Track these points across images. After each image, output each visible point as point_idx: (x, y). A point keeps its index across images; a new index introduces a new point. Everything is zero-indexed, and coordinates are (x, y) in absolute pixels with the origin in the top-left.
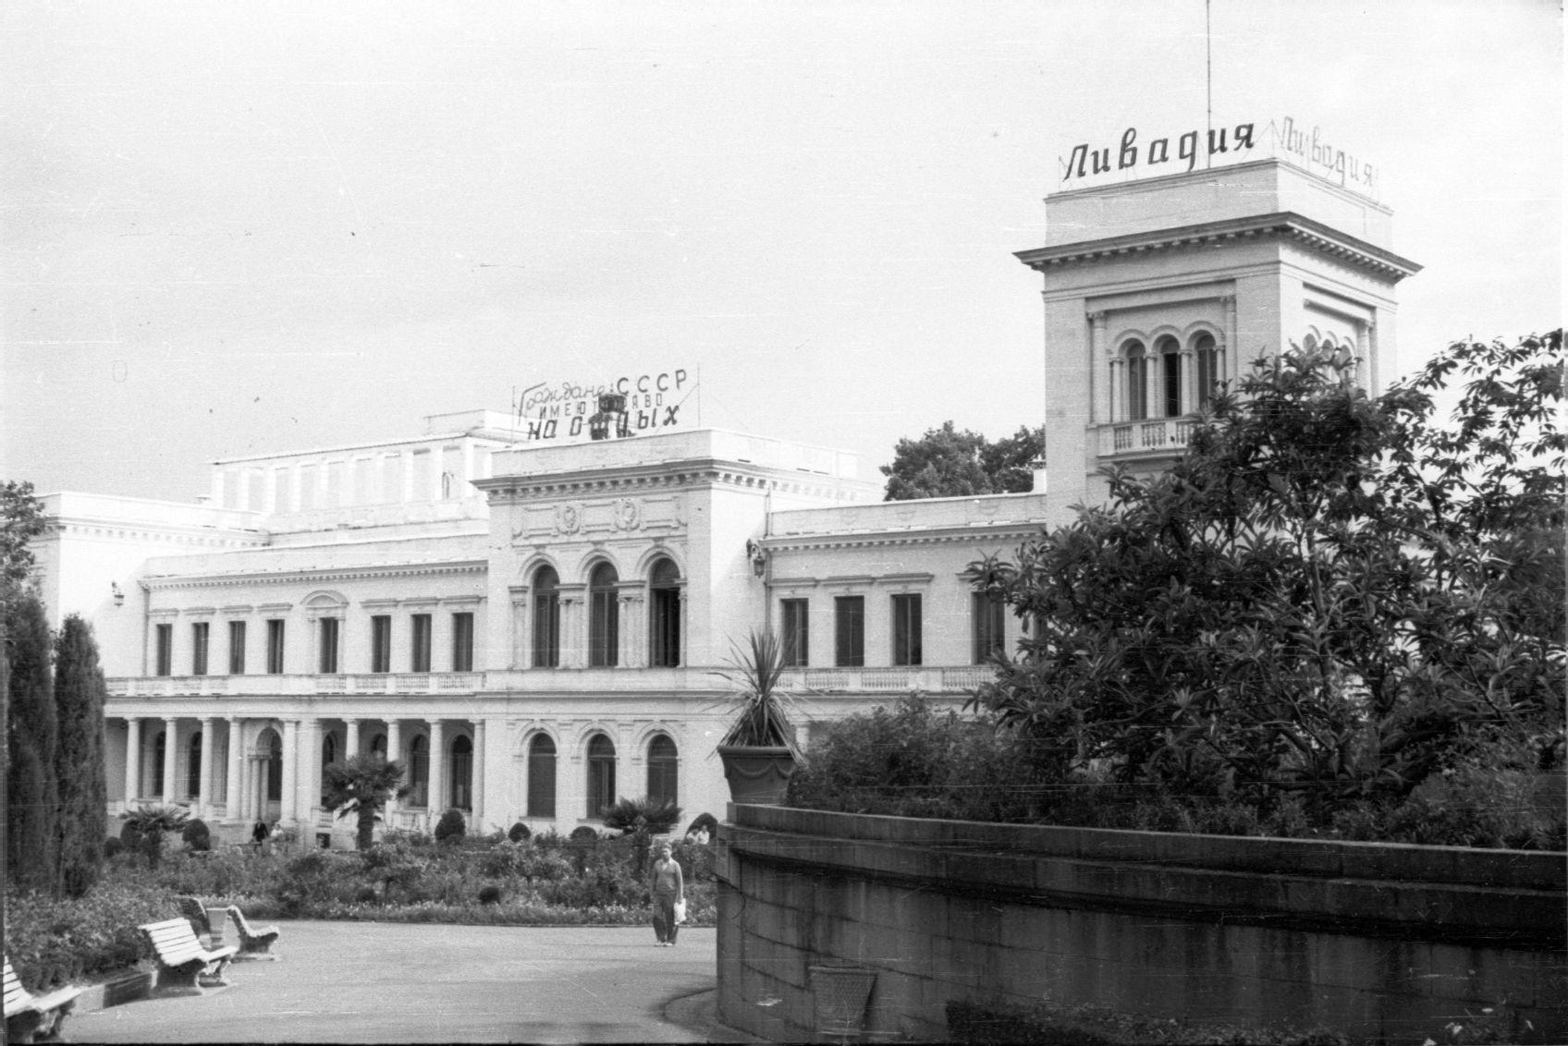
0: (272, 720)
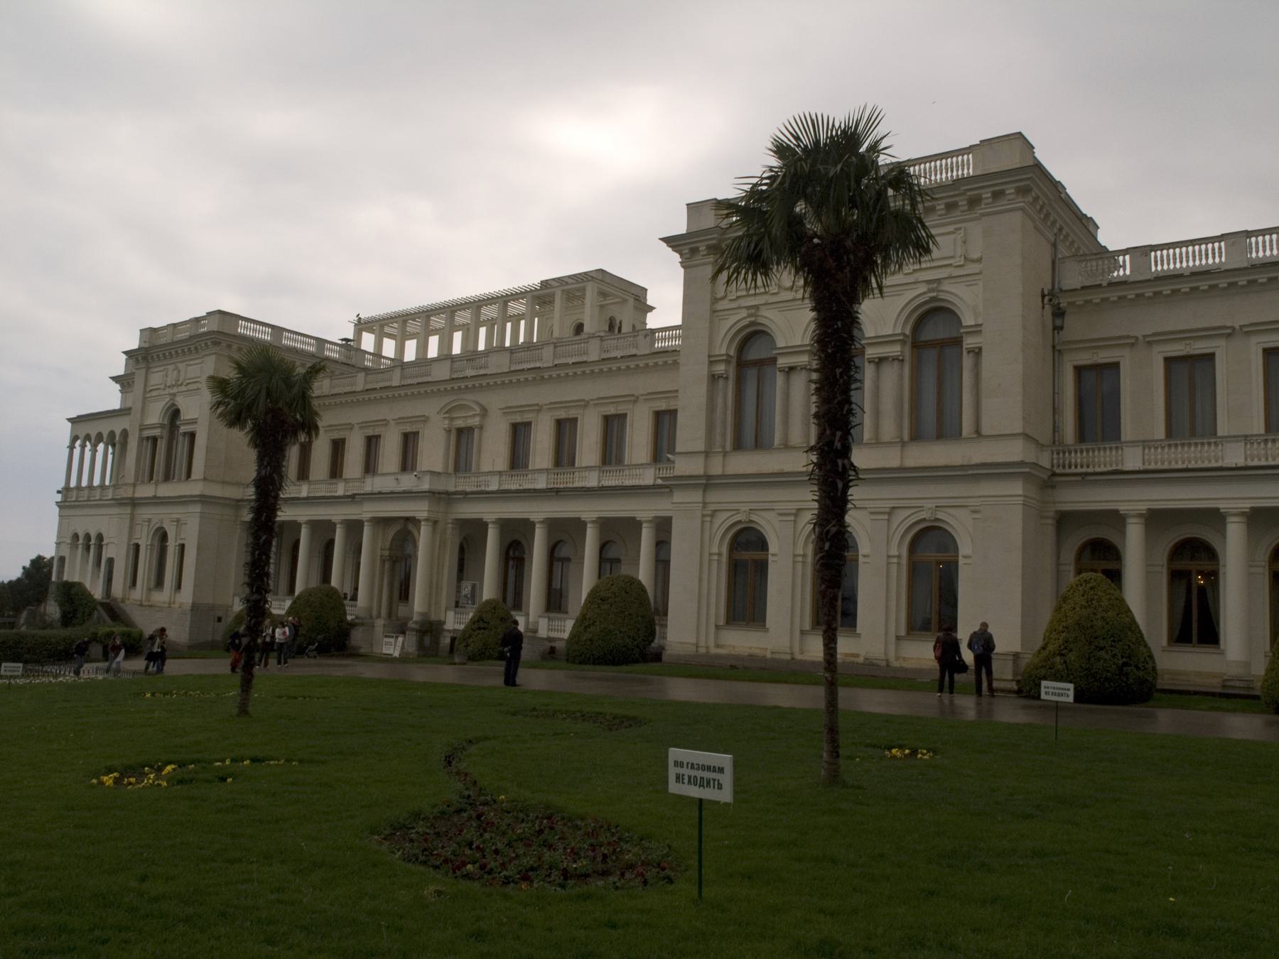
0: (407, 519)
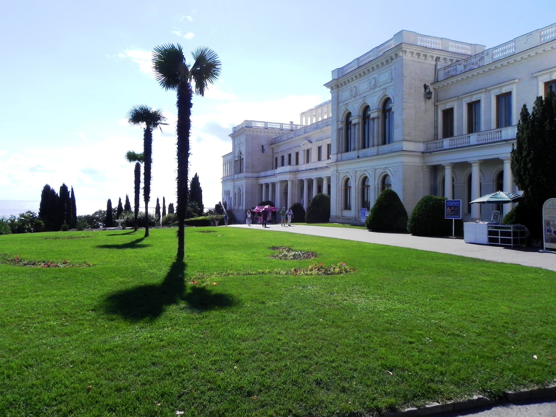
0: (287, 181)
